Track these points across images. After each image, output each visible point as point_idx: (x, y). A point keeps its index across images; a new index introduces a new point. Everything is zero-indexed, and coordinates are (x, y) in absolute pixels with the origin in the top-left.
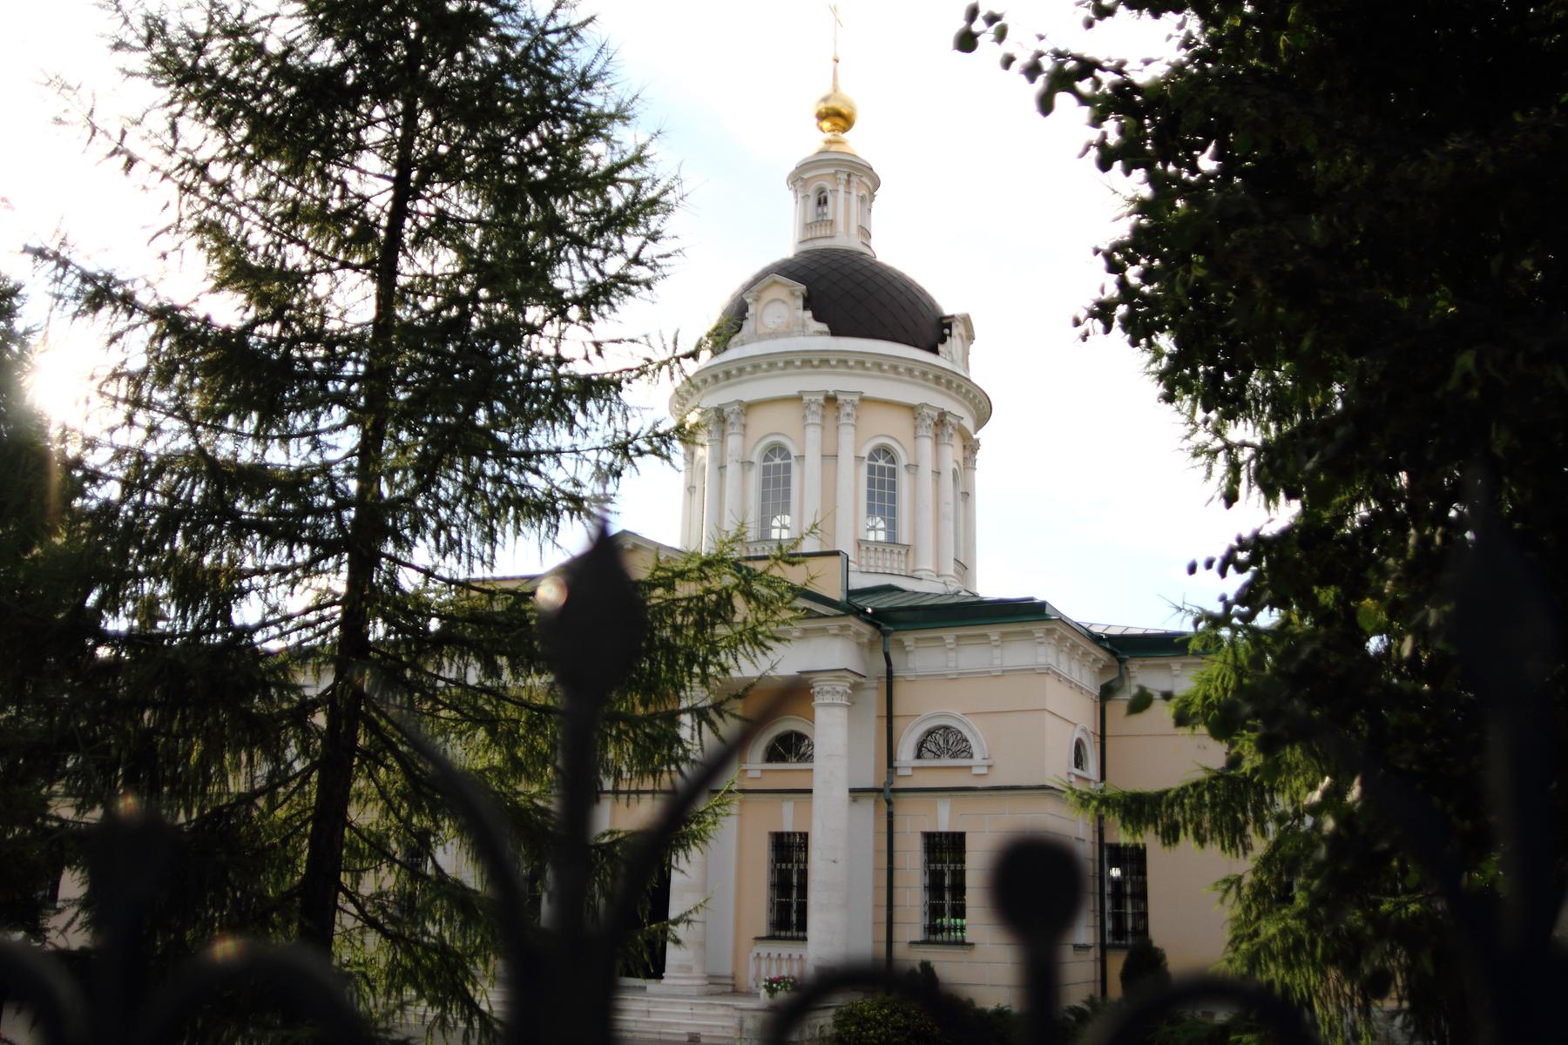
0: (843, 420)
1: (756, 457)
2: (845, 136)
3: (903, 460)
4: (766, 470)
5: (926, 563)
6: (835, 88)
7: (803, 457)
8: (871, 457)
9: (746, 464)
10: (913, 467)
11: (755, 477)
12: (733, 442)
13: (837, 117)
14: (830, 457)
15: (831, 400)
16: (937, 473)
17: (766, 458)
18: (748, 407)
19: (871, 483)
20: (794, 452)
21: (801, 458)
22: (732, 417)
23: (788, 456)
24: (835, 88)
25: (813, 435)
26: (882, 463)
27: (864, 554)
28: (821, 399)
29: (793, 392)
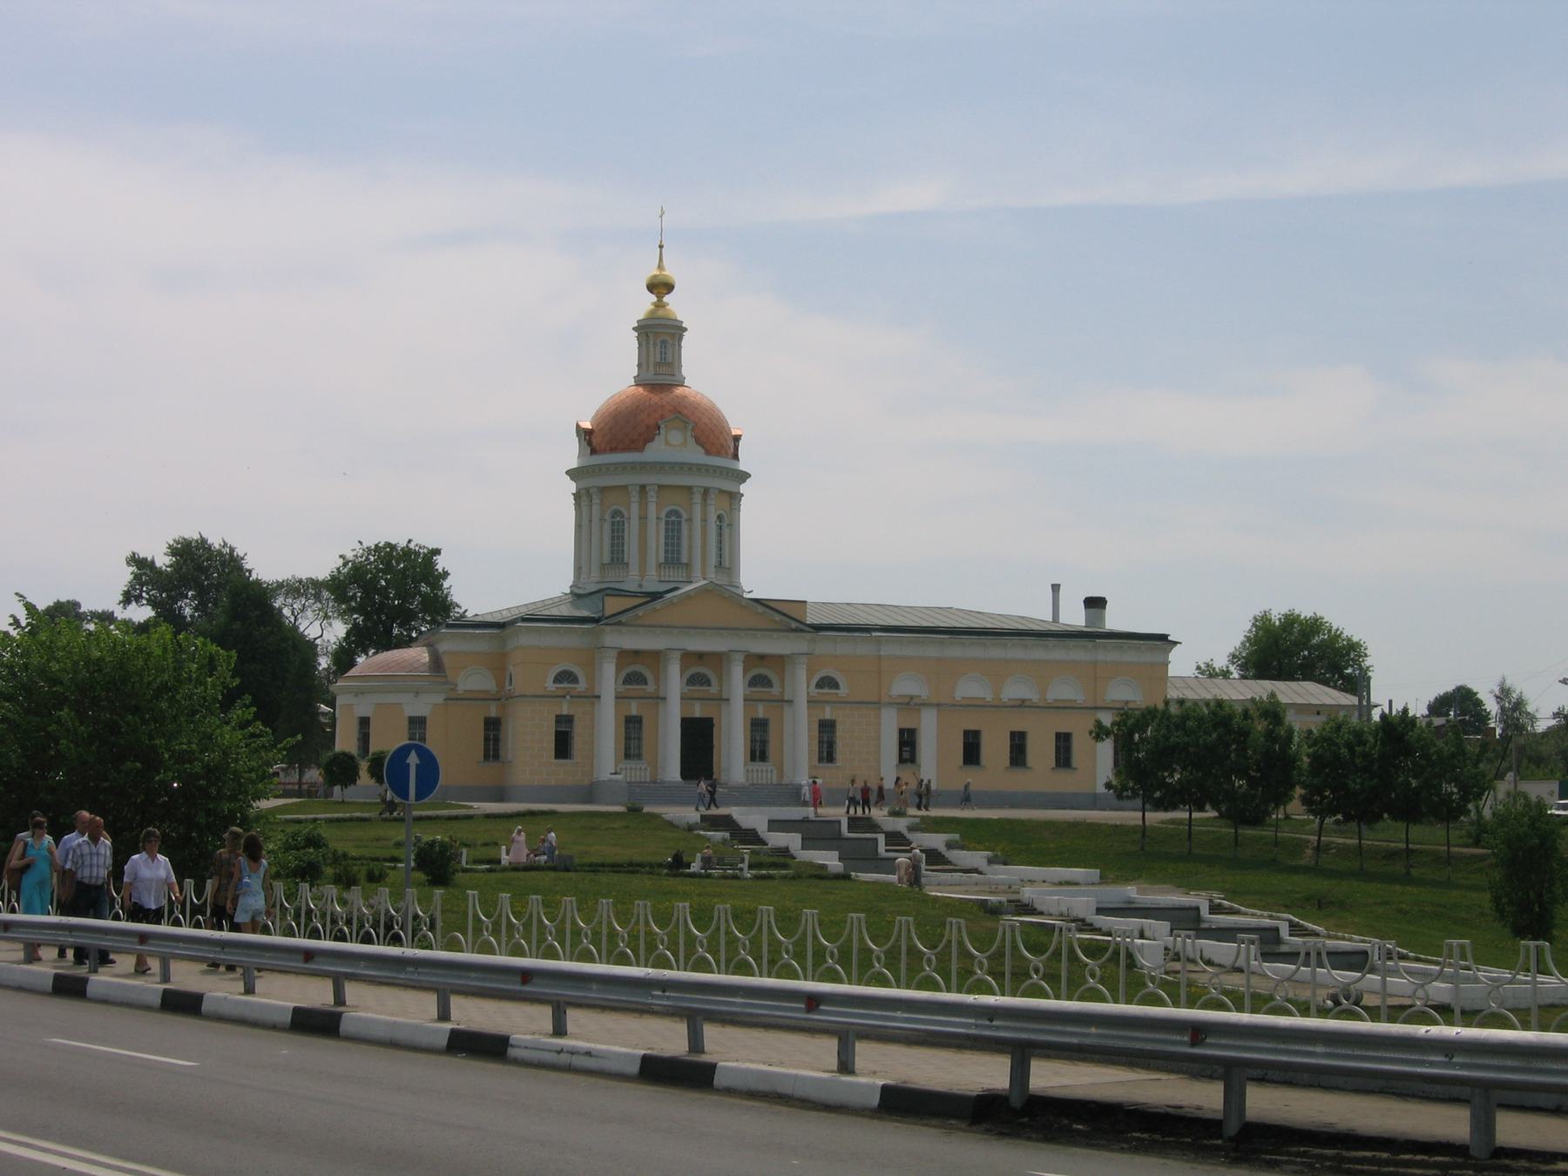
2: (666, 299)
3: (685, 516)
4: (613, 523)
7: (630, 518)
8: (667, 516)
9: (602, 520)
10: (690, 520)
11: (607, 527)
12: (596, 508)
13: (661, 287)
14: (643, 518)
15: (643, 488)
16: (704, 520)
17: (613, 517)
19: (667, 530)
20: (626, 516)
23: (623, 516)
26: (673, 518)
27: (662, 570)
28: (638, 488)
29: (623, 484)
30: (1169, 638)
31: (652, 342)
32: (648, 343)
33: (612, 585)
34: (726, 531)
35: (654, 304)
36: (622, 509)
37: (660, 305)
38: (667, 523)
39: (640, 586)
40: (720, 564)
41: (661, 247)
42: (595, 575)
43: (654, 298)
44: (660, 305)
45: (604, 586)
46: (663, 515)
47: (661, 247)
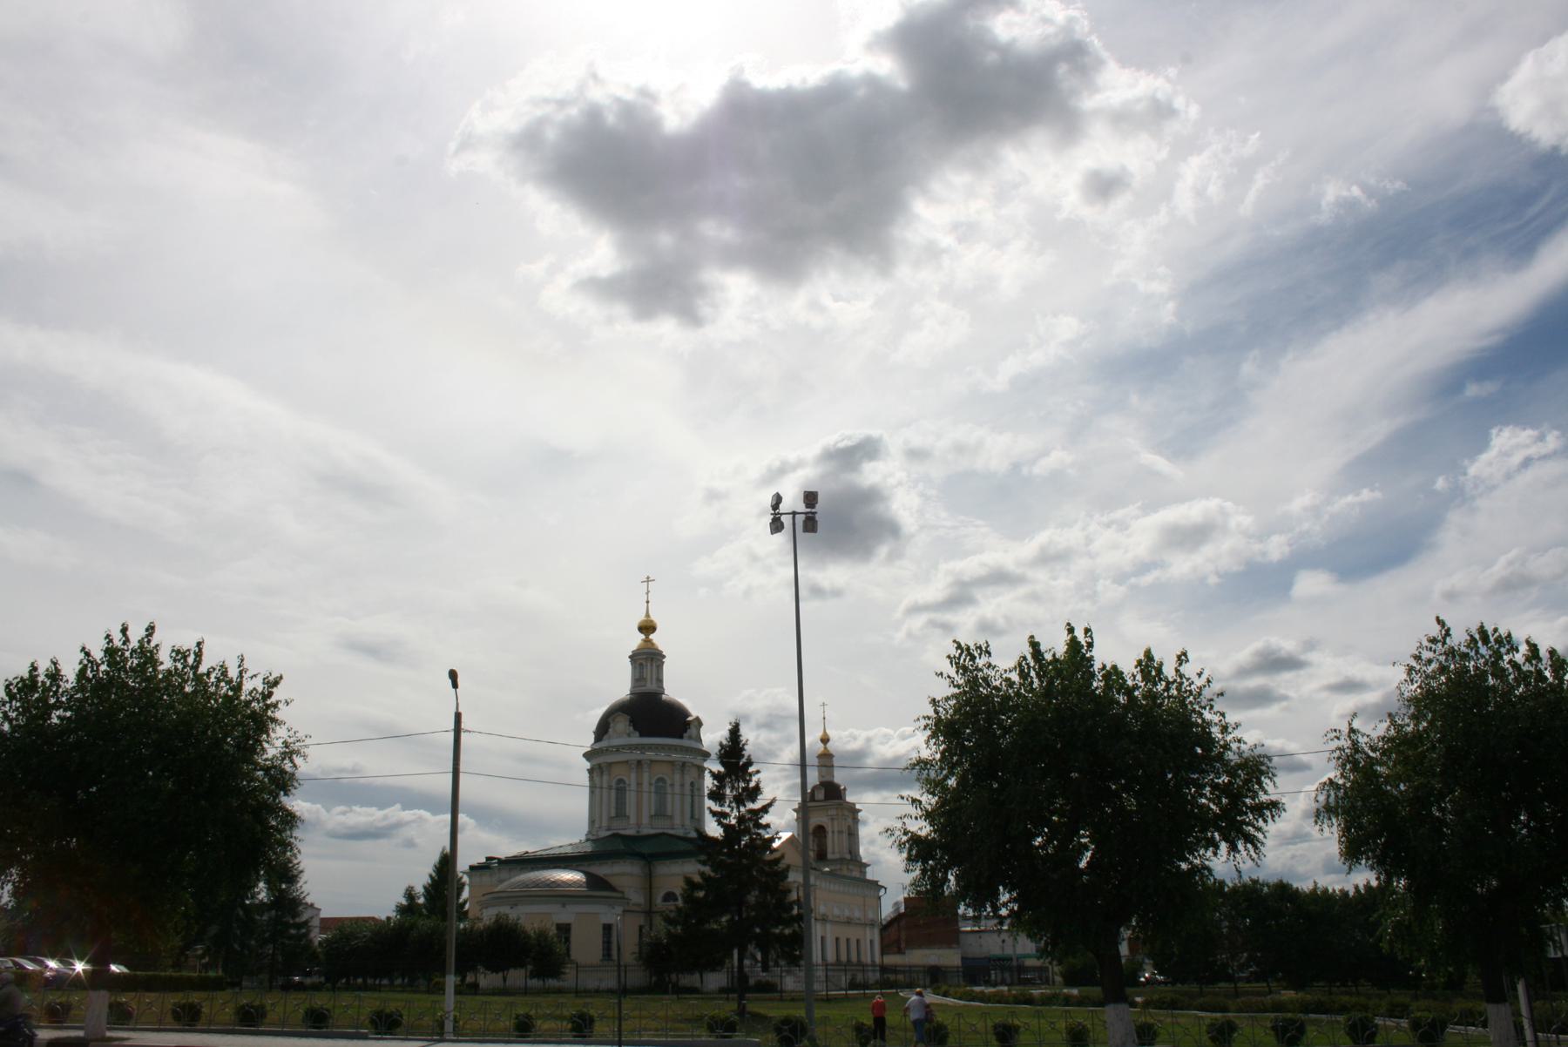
0: (686, 772)
1: (653, 781)
2: (651, 637)
3: (696, 787)
5: (677, 821)
6: (648, 615)
9: (650, 784)
12: (646, 776)
14: (682, 785)
15: (684, 764)
17: (656, 783)
18: (652, 761)
20: (669, 782)
21: (672, 785)
22: (646, 766)
24: (648, 615)
25: (677, 777)
30: (880, 883)
31: (654, 665)
32: (652, 665)
33: (666, 831)
34: (696, 798)
35: (642, 640)
36: (666, 778)
37: (647, 641)
38: (617, 789)
39: (638, 832)
40: (692, 817)
41: (648, 602)
42: (645, 820)
43: (643, 637)
44: (647, 637)
45: (661, 831)
46: (614, 784)
47: (648, 602)
